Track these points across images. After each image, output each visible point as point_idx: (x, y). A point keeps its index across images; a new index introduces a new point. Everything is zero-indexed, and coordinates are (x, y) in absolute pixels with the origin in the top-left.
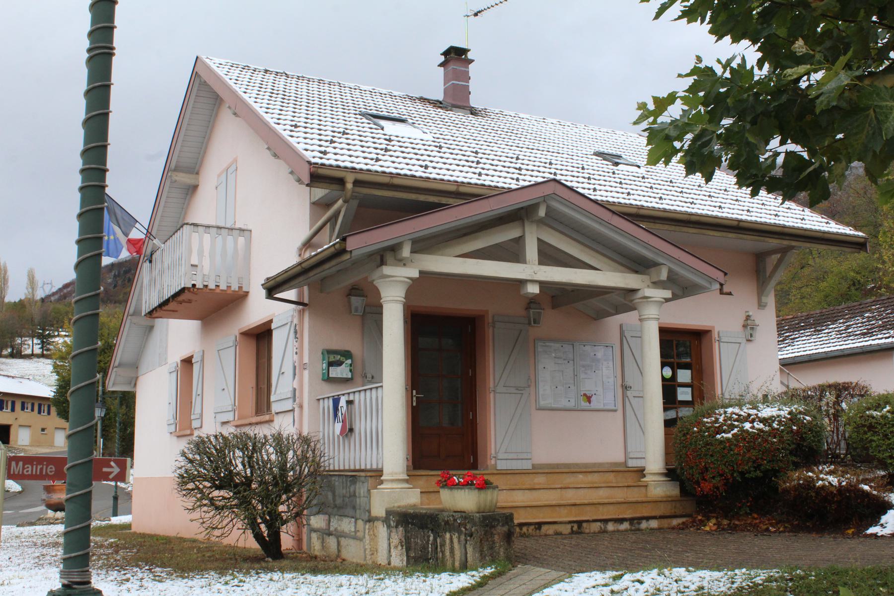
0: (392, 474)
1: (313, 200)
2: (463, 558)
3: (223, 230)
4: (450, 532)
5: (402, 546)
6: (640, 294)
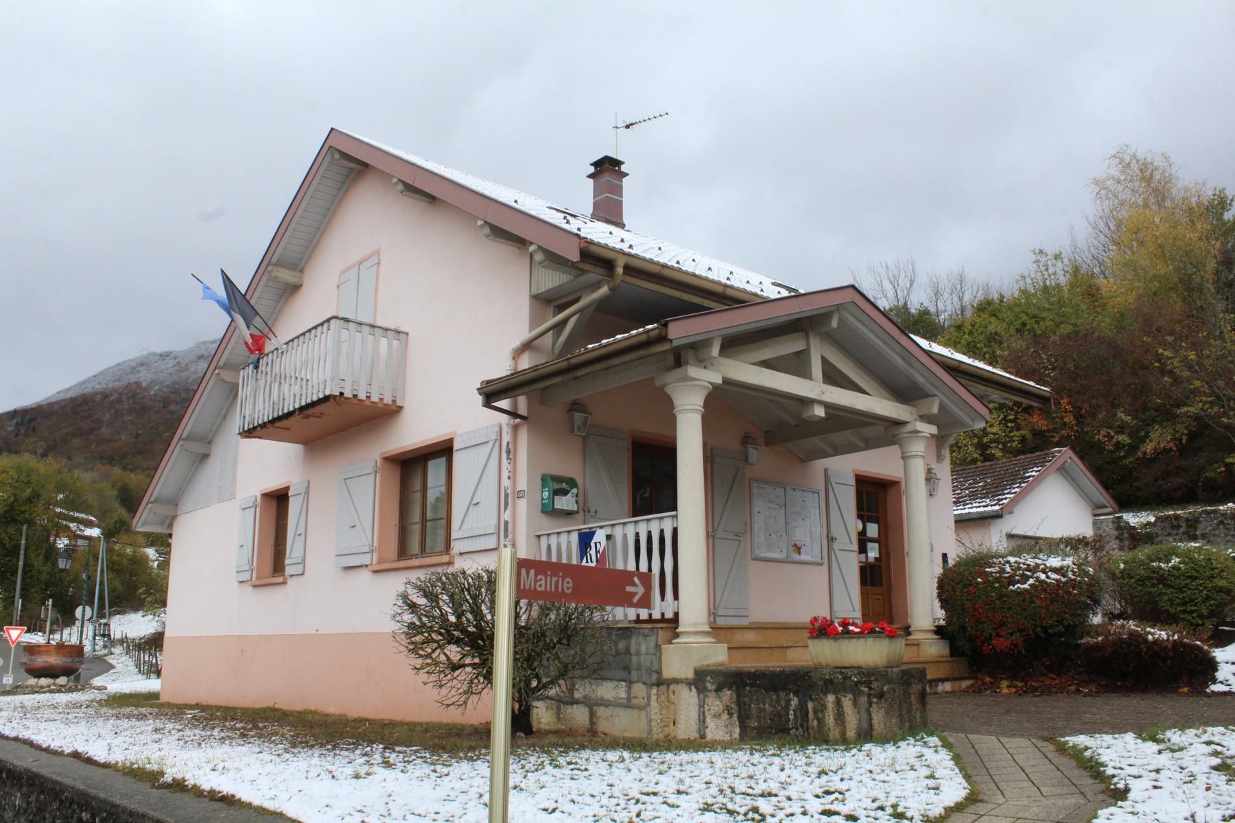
0: (695, 625)
1: (535, 292)
2: (865, 725)
4: (835, 692)
5: (731, 715)
6: (909, 428)
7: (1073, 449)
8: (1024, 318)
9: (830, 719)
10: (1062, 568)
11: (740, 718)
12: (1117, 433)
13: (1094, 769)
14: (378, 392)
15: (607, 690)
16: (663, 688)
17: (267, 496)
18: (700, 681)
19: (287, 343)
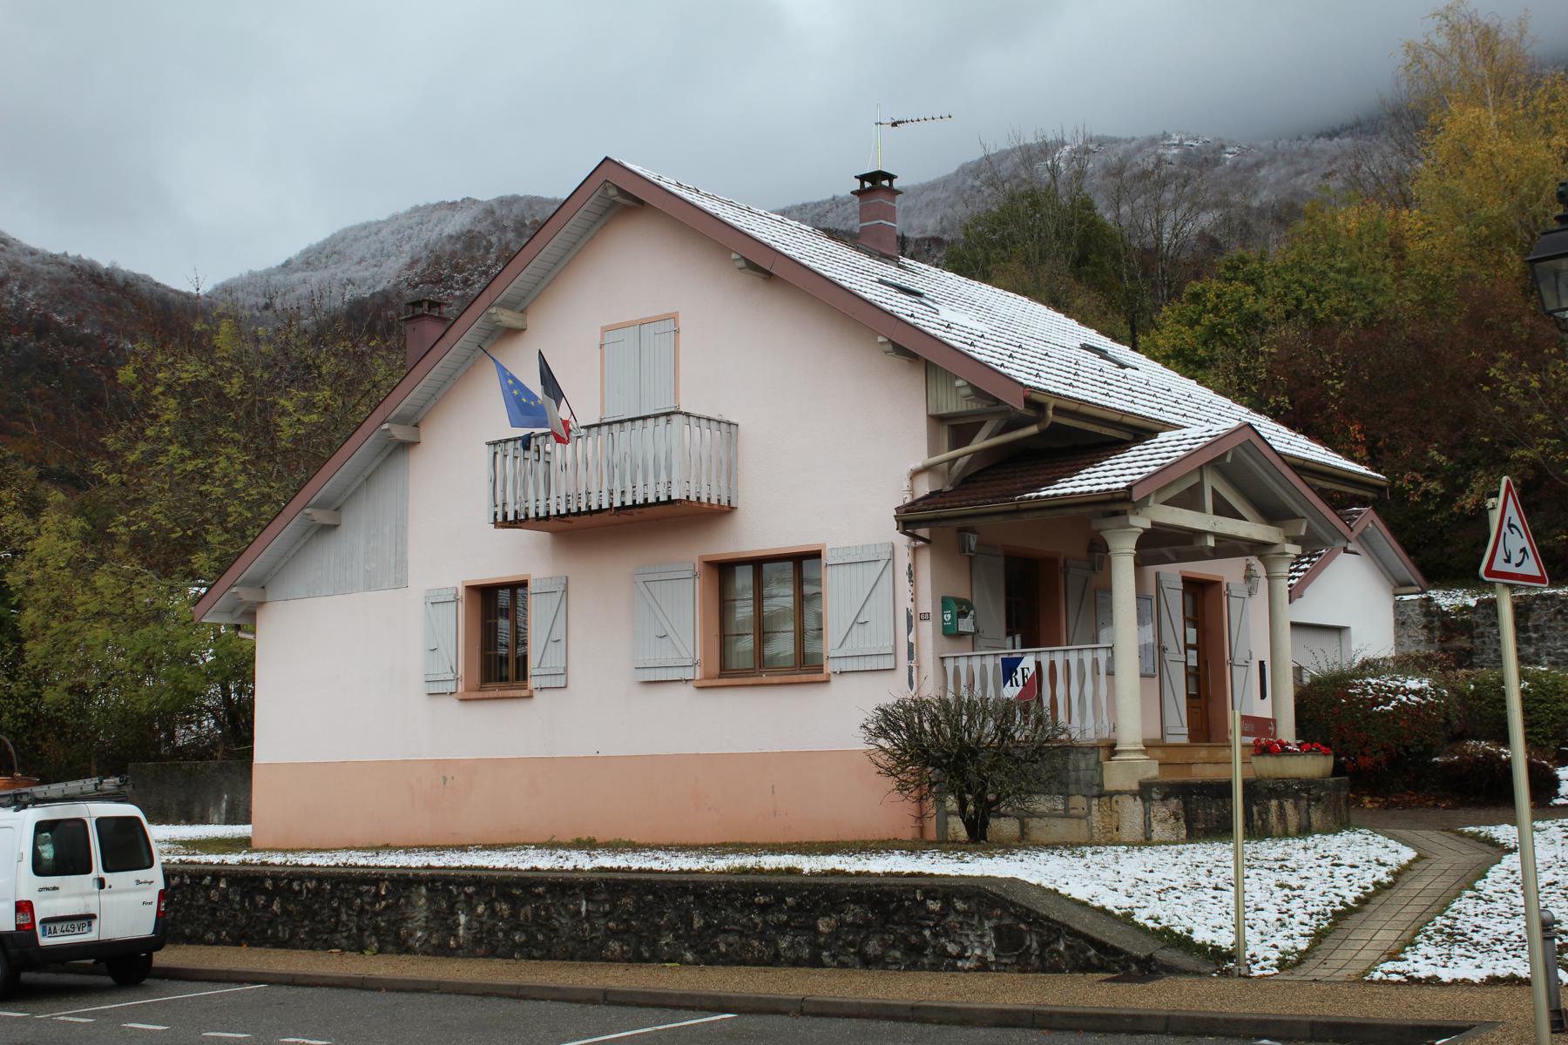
0: (1135, 744)
1: (933, 411)
2: (1305, 823)
3: (674, 418)
5: (1177, 819)
7: (1375, 509)
8: (1301, 292)
9: (1273, 818)
10: (1421, 690)
11: (1186, 822)
12: (1426, 477)
13: (1491, 842)
14: (709, 491)
15: (1042, 803)
16: (1106, 799)
17: (473, 589)
18: (1145, 791)
19: (588, 427)
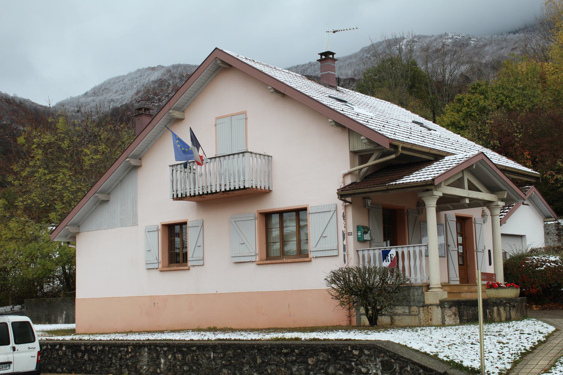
0: (437, 285)
1: (352, 149)
2: (508, 316)
3: (246, 154)
4: (497, 306)
5: (456, 316)
6: (495, 204)
7: (536, 187)
8: (503, 98)
9: (495, 315)
10: (556, 261)
12: (556, 173)
14: (259, 183)
15: (399, 310)
16: (426, 308)
17: (164, 226)
18: (442, 304)
19: (211, 159)
